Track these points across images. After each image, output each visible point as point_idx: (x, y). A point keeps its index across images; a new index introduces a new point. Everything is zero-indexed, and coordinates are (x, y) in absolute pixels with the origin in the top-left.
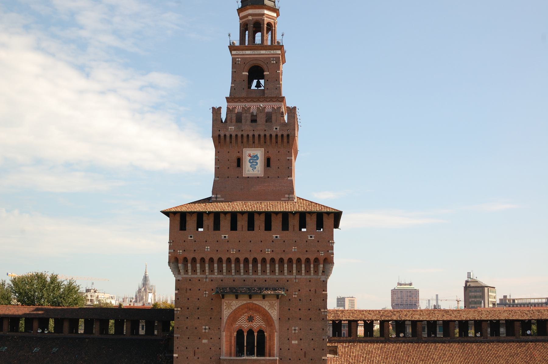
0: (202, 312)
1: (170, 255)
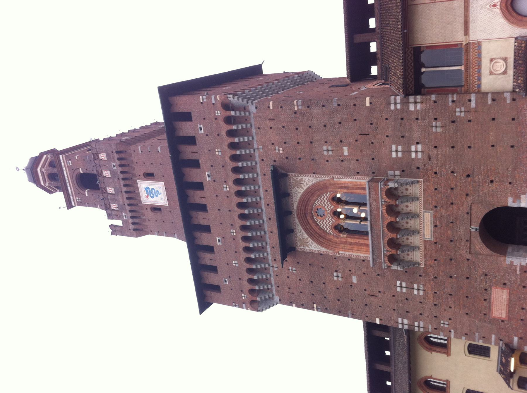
0: (315, 277)
1: (249, 308)
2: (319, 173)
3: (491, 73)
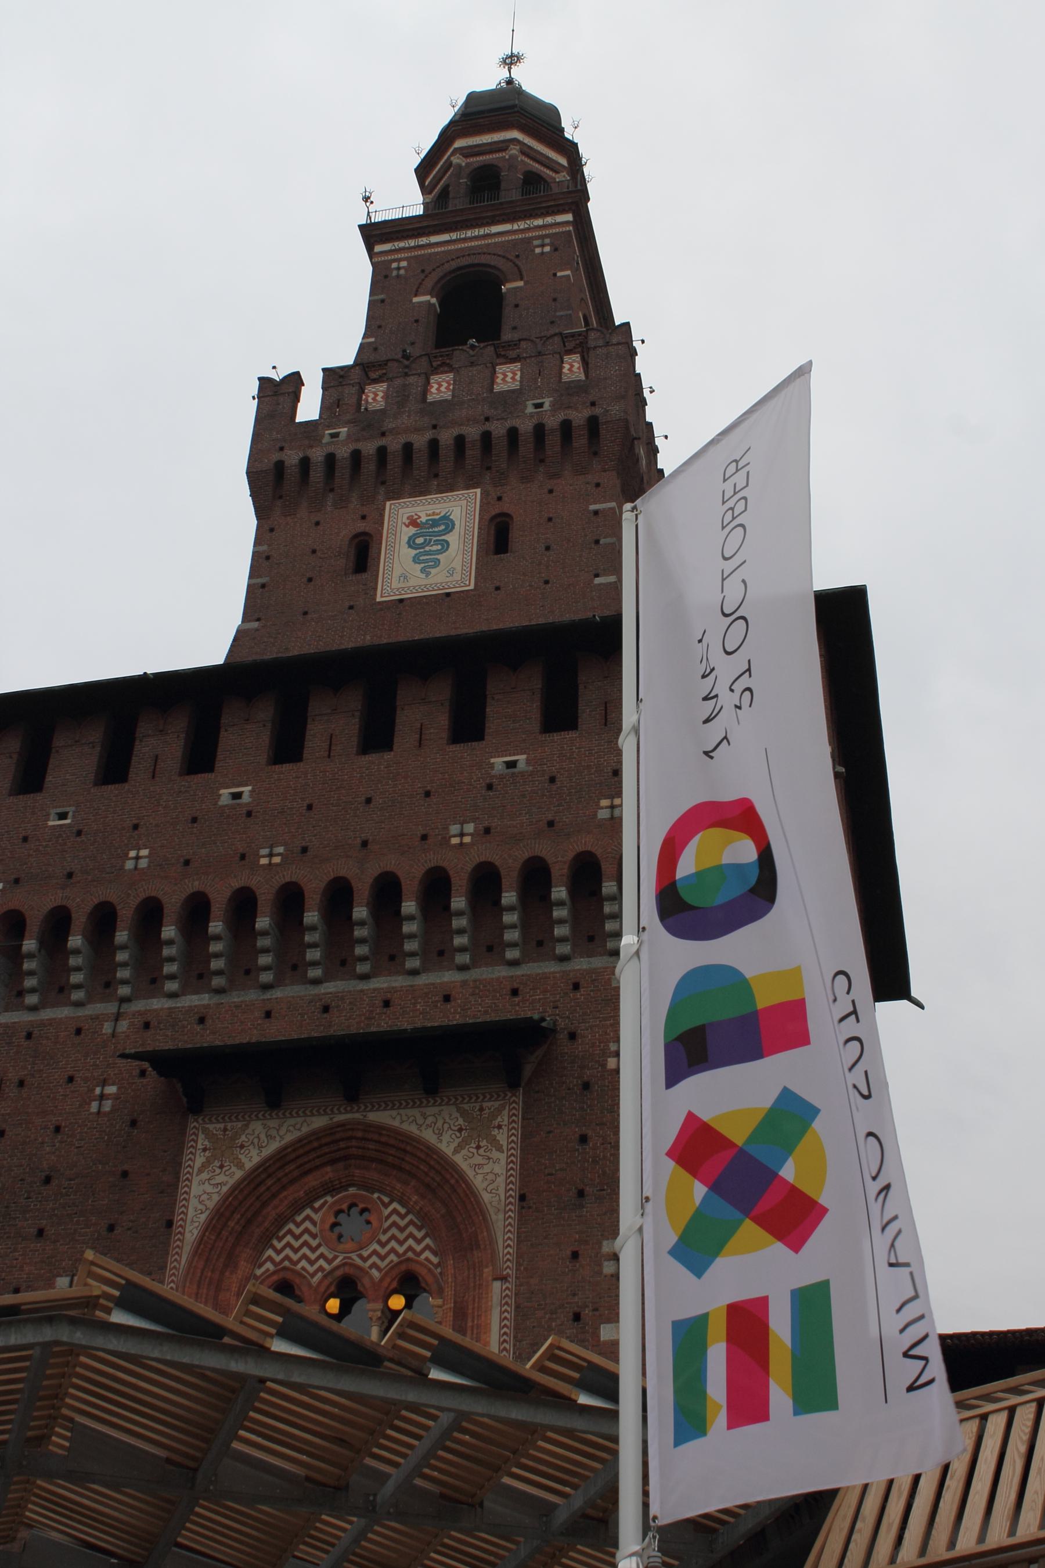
2: (522, 1220)
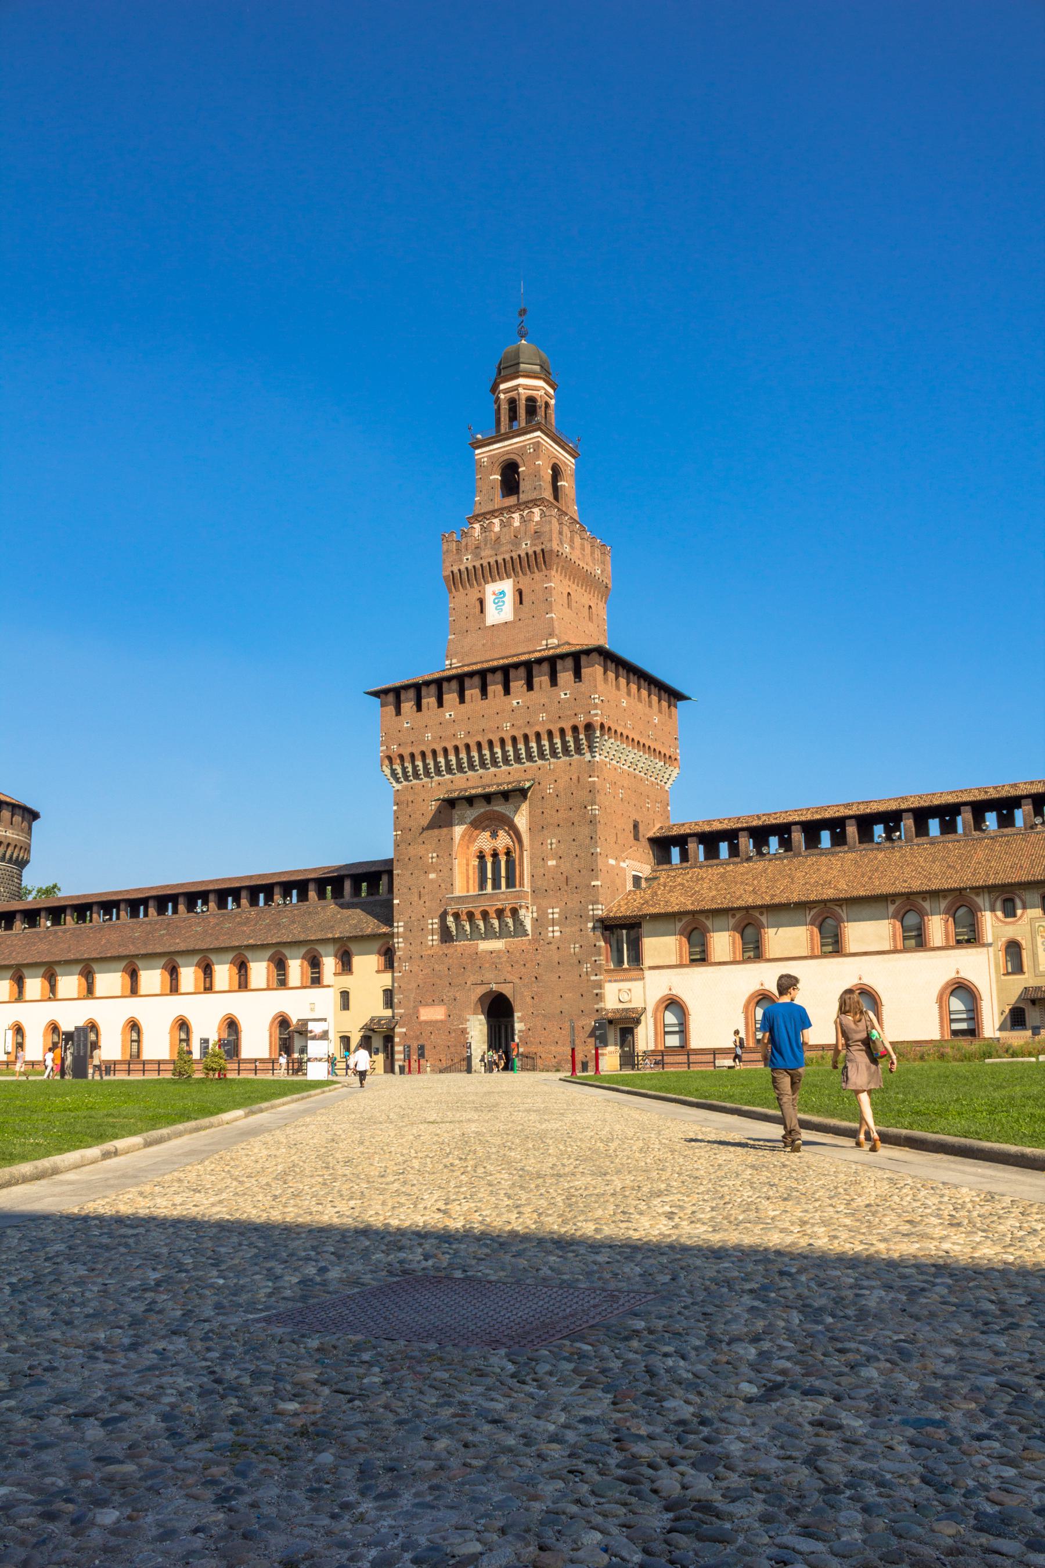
3: (620, 990)
